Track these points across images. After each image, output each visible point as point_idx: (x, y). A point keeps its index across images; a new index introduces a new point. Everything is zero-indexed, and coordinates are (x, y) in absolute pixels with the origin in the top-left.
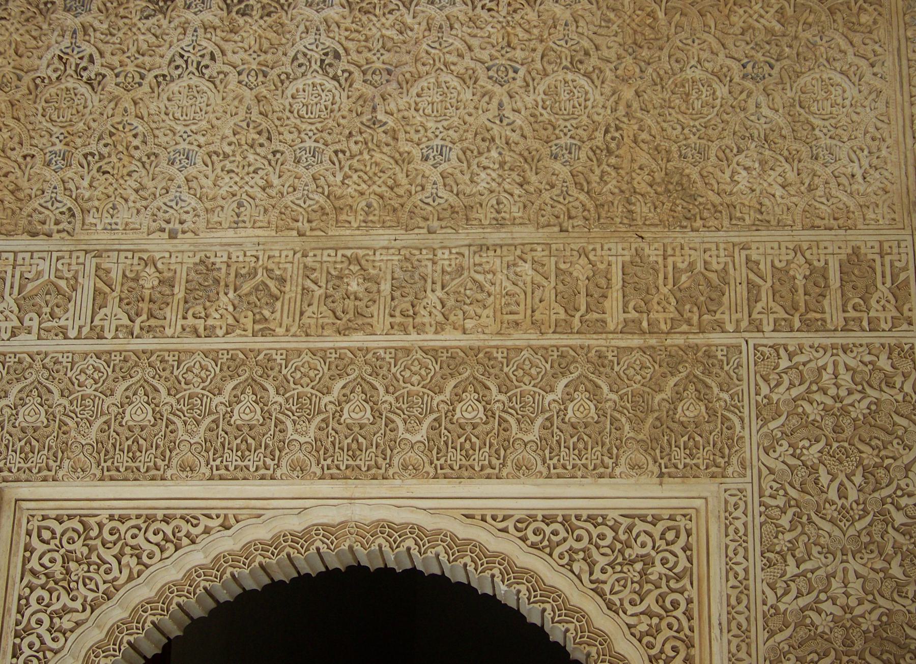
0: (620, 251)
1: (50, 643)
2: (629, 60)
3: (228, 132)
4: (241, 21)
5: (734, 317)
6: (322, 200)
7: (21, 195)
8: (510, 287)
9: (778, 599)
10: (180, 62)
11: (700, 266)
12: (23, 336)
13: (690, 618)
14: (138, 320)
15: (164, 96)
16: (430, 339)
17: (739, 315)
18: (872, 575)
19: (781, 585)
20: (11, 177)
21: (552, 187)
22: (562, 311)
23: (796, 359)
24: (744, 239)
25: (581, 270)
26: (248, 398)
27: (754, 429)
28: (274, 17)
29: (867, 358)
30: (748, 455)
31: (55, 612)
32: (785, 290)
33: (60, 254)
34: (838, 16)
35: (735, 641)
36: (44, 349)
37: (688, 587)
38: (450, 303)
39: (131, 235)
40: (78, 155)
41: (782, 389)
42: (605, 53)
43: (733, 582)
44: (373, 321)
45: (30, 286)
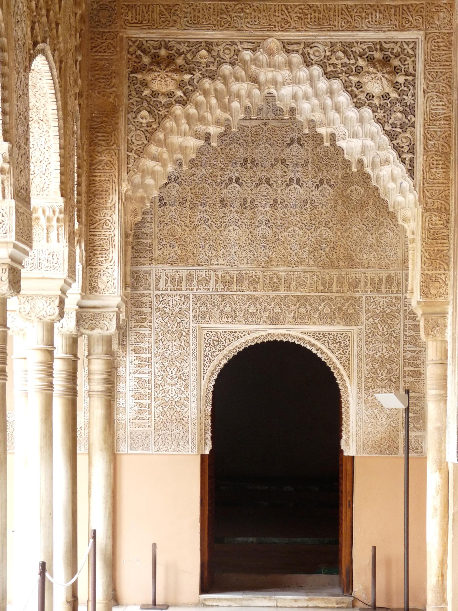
2: (339, 224)
3: (244, 241)
4: (245, 211)
7: (195, 255)
8: (311, 282)
10: (230, 221)
11: (354, 277)
12: (199, 290)
14: (226, 287)
15: (227, 230)
16: (293, 293)
21: (321, 257)
25: (327, 278)
26: (253, 306)
28: (253, 210)
29: (390, 300)
32: (373, 283)
34: (389, 214)
38: (298, 285)
39: (222, 266)
41: (371, 306)
42: (334, 222)
45: (200, 279)
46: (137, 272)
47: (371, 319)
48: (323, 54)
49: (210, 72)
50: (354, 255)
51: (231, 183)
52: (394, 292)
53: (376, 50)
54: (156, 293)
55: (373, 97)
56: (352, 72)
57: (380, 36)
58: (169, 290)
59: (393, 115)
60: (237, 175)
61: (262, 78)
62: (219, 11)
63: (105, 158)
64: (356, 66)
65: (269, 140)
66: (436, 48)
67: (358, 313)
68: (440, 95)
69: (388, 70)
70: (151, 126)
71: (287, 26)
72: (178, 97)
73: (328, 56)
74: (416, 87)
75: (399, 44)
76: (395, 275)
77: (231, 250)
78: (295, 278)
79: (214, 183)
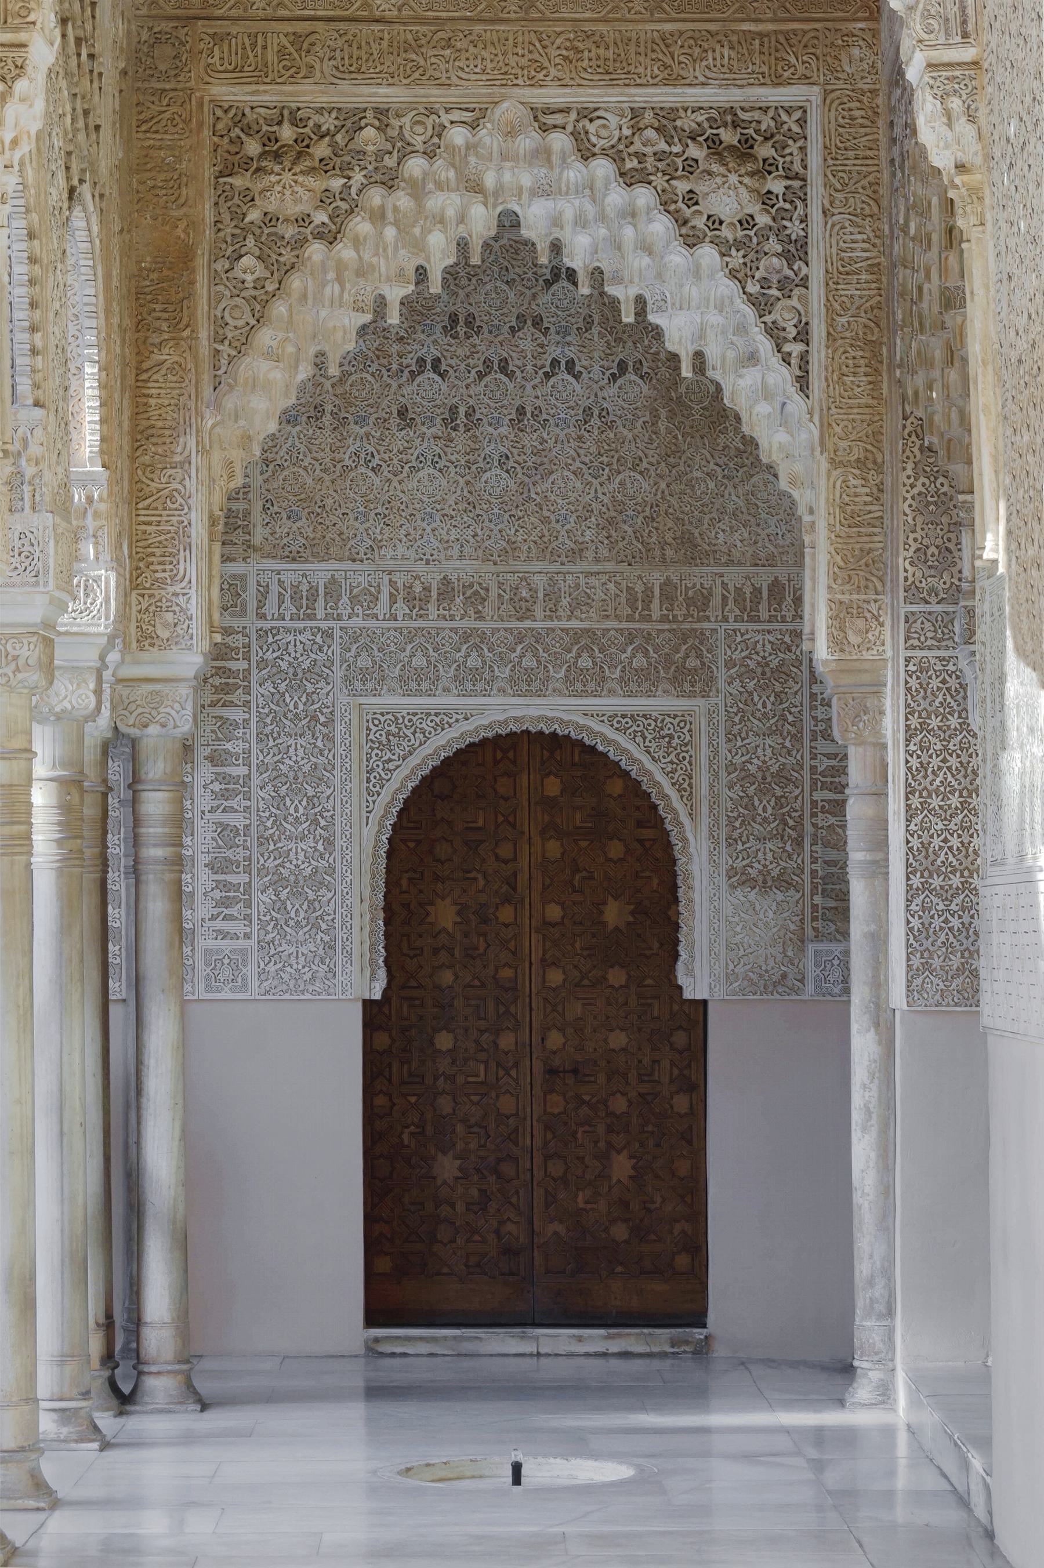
5: (716, 614)
6: (505, 544)
8: (604, 597)
10: (422, 459)
11: (698, 586)
15: (416, 480)
18: (777, 746)
19: (734, 750)
21: (624, 539)
25: (639, 588)
26: (474, 654)
27: (724, 672)
29: (779, 637)
40: (372, 515)
41: (737, 652)
43: (712, 749)
45: (355, 591)
47: (737, 683)
48: (617, 133)
49: (385, 171)
51: (423, 372)
53: (725, 125)
54: (259, 626)
55: (721, 223)
56: (676, 170)
57: (733, 96)
58: (288, 618)
59: (763, 261)
60: (435, 352)
61: (490, 180)
62: (402, 45)
63: (168, 357)
64: (684, 157)
65: (504, 272)
66: (847, 121)
67: (709, 667)
68: (858, 220)
69: (750, 169)
70: (263, 287)
71: (541, 76)
72: (317, 226)
73: (627, 138)
74: (809, 202)
75: (771, 113)
76: (789, 581)
77: (424, 525)
78: (567, 589)
79: (384, 371)
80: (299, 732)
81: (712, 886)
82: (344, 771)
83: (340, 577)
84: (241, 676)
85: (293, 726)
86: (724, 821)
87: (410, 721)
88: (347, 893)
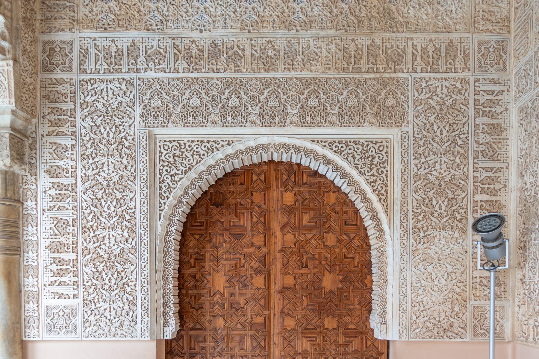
0: (367, 40)
1: (171, 185)
5: (407, 67)
8: (327, 54)
9: (418, 170)
11: (395, 47)
12: (149, 71)
13: (387, 177)
14: (192, 66)
16: (298, 74)
17: (409, 66)
19: (419, 165)
20: (137, 6)
21: (342, 14)
22: (346, 64)
23: (428, 83)
24: (411, 36)
25: (352, 48)
26: (234, 97)
27: (413, 109)
29: (453, 83)
30: (410, 119)
31: (173, 175)
32: (425, 56)
33: (159, 38)
35: (403, 185)
36: (157, 77)
37: (387, 166)
39: (185, 31)
41: (423, 94)
43: (403, 164)
44: (278, 67)
45: (149, 51)
46: (52, 42)
50: (394, 10)
52: (459, 71)
54: (82, 78)
78: (301, 49)
80: (110, 153)
81: (402, 262)
82: (142, 181)
83: (138, 43)
84: (69, 114)
85: (106, 149)
86: (411, 215)
87: (189, 146)
88: (145, 266)
